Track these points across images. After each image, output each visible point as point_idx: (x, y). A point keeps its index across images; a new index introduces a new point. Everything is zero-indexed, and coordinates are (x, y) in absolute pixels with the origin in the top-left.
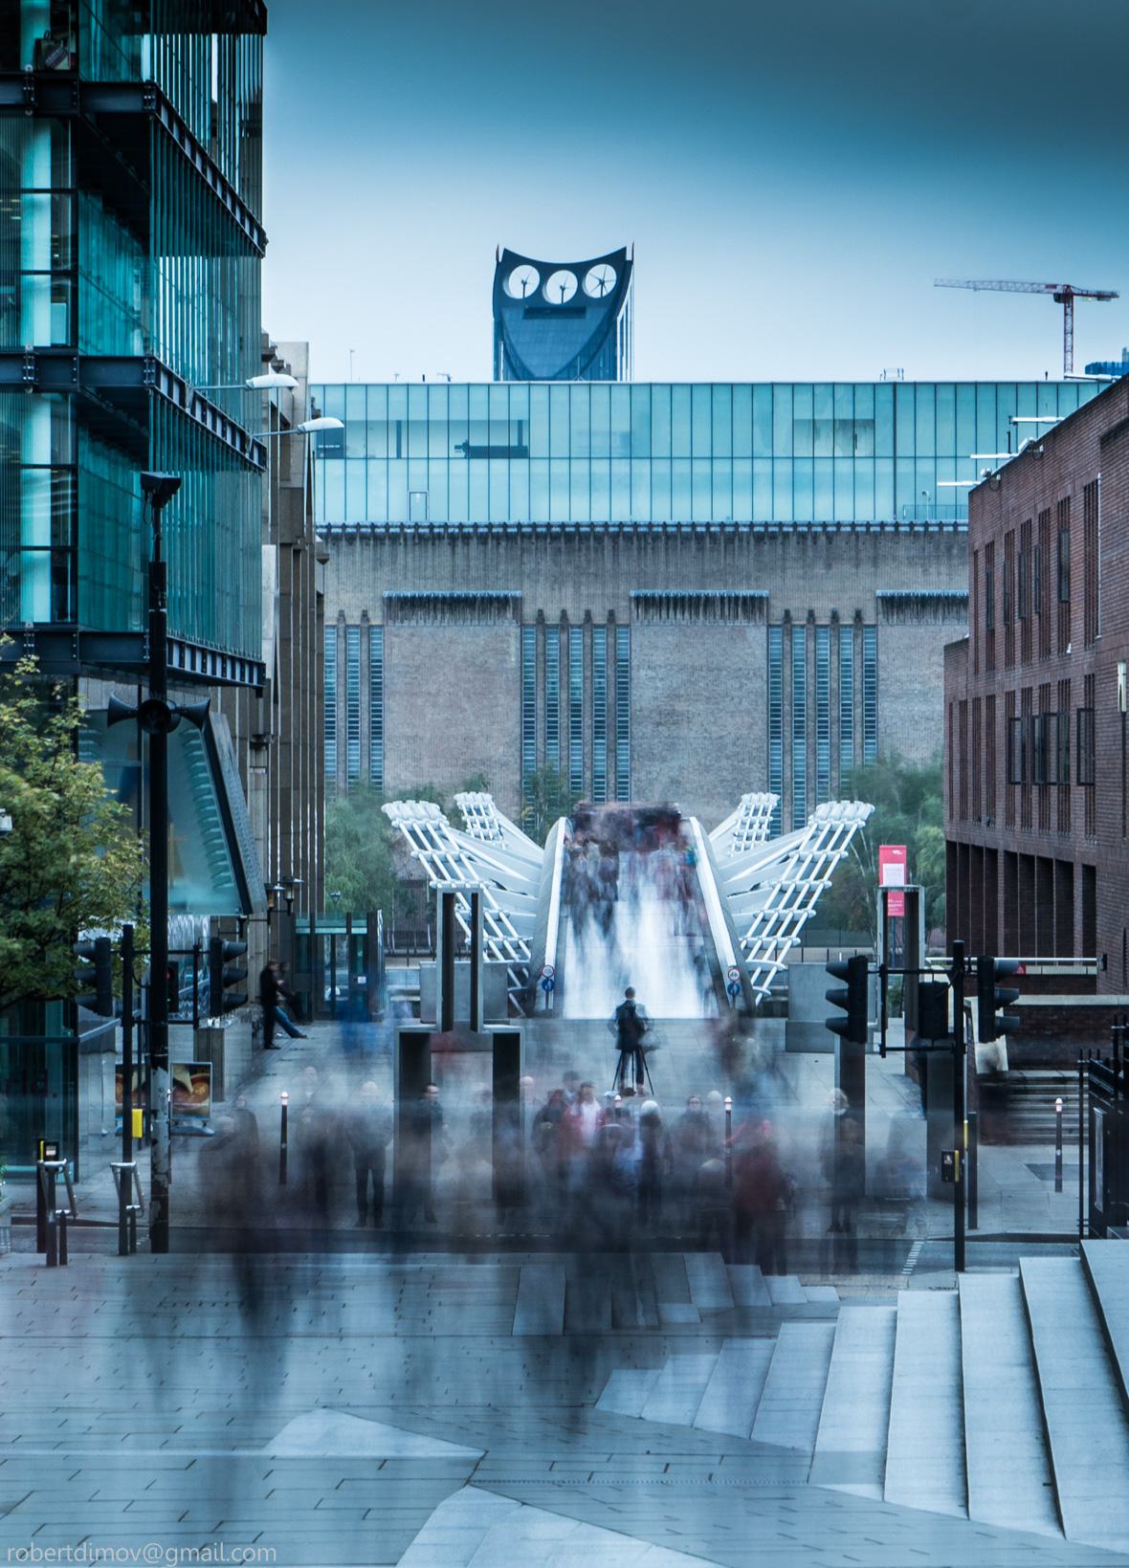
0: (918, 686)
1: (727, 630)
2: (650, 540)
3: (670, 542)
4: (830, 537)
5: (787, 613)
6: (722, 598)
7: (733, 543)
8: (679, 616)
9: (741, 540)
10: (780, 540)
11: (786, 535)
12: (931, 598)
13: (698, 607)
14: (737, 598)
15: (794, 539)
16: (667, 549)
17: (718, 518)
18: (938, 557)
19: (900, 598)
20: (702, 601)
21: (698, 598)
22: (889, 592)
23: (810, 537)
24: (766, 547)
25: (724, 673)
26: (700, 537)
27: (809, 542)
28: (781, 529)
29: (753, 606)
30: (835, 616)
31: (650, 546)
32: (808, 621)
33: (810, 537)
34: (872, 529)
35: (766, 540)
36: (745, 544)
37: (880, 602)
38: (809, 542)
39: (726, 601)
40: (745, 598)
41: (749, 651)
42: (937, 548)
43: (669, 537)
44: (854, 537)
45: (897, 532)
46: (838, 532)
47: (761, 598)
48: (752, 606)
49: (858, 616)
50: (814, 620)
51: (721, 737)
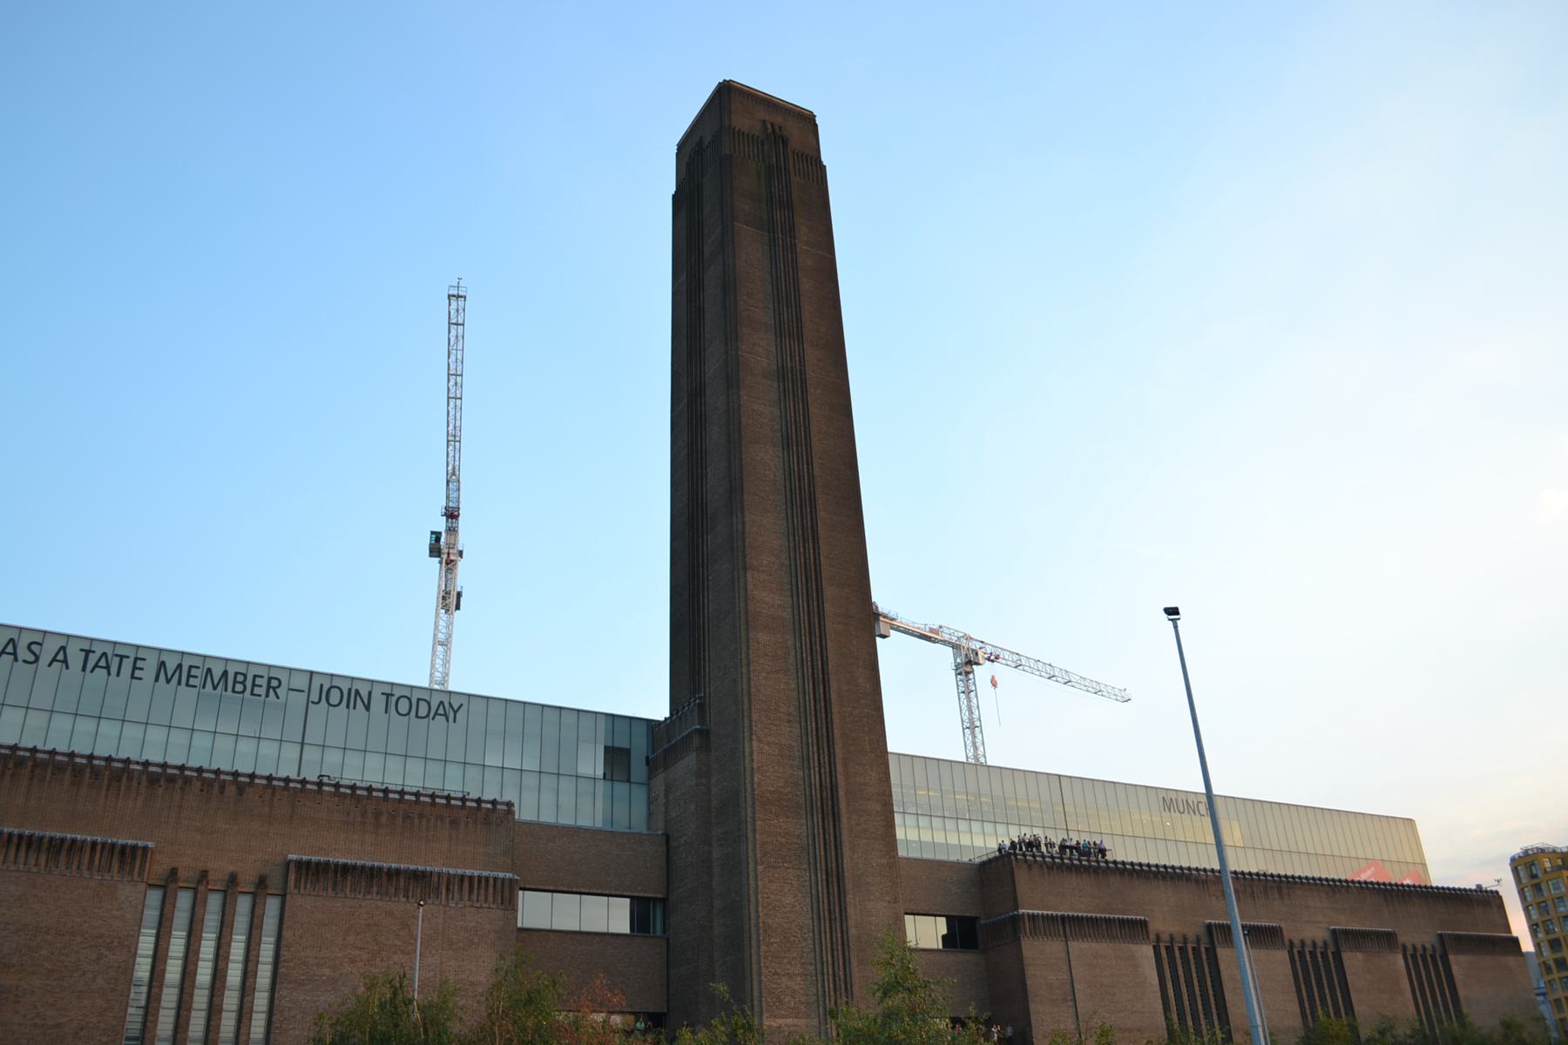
0: (327, 972)
1: (92, 884)
2: (11, 765)
3: (37, 771)
4: (241, 788)
5: (173, 873)
6: (94, 844)
7: (119, 781)
8: (32, 861)
9: (130, 779)
10: (180, 782)
11: (187, 781)
12: (354, 867)
13: (59, 852)
14: (113, 845)
15: (198, 784)
16: (31, 778)
17: (102, 751)
18: (364, 823)
19: (318, 864)
20: (66, 844)
21: (63, 840)
22: (305, 858)
23: (216, 785)
24: (161, 791)
25: (79, 939)
26: (77, 771)
27: (216, 791)
28: (182, 772)
29: (134, 857)
30: (233, 880)
31: (9, 773)
32: (200, 882)
33: (216, 785)
34: (291, 785)
35: (162, 783)
36: (134, 783)
37: (292, 866)
38: (216, 791)
39: (99, 847)
40: (124, 847)
41: (115, 912)
42: (364, 814)
43: (38, 765)
44: (270, 791)
45: (320, 791)
46: (251, 784)
47: (145, 849)
48: (129, 857)
49: (262, 882)
50: (208, 883)
51: (59, 1025)
